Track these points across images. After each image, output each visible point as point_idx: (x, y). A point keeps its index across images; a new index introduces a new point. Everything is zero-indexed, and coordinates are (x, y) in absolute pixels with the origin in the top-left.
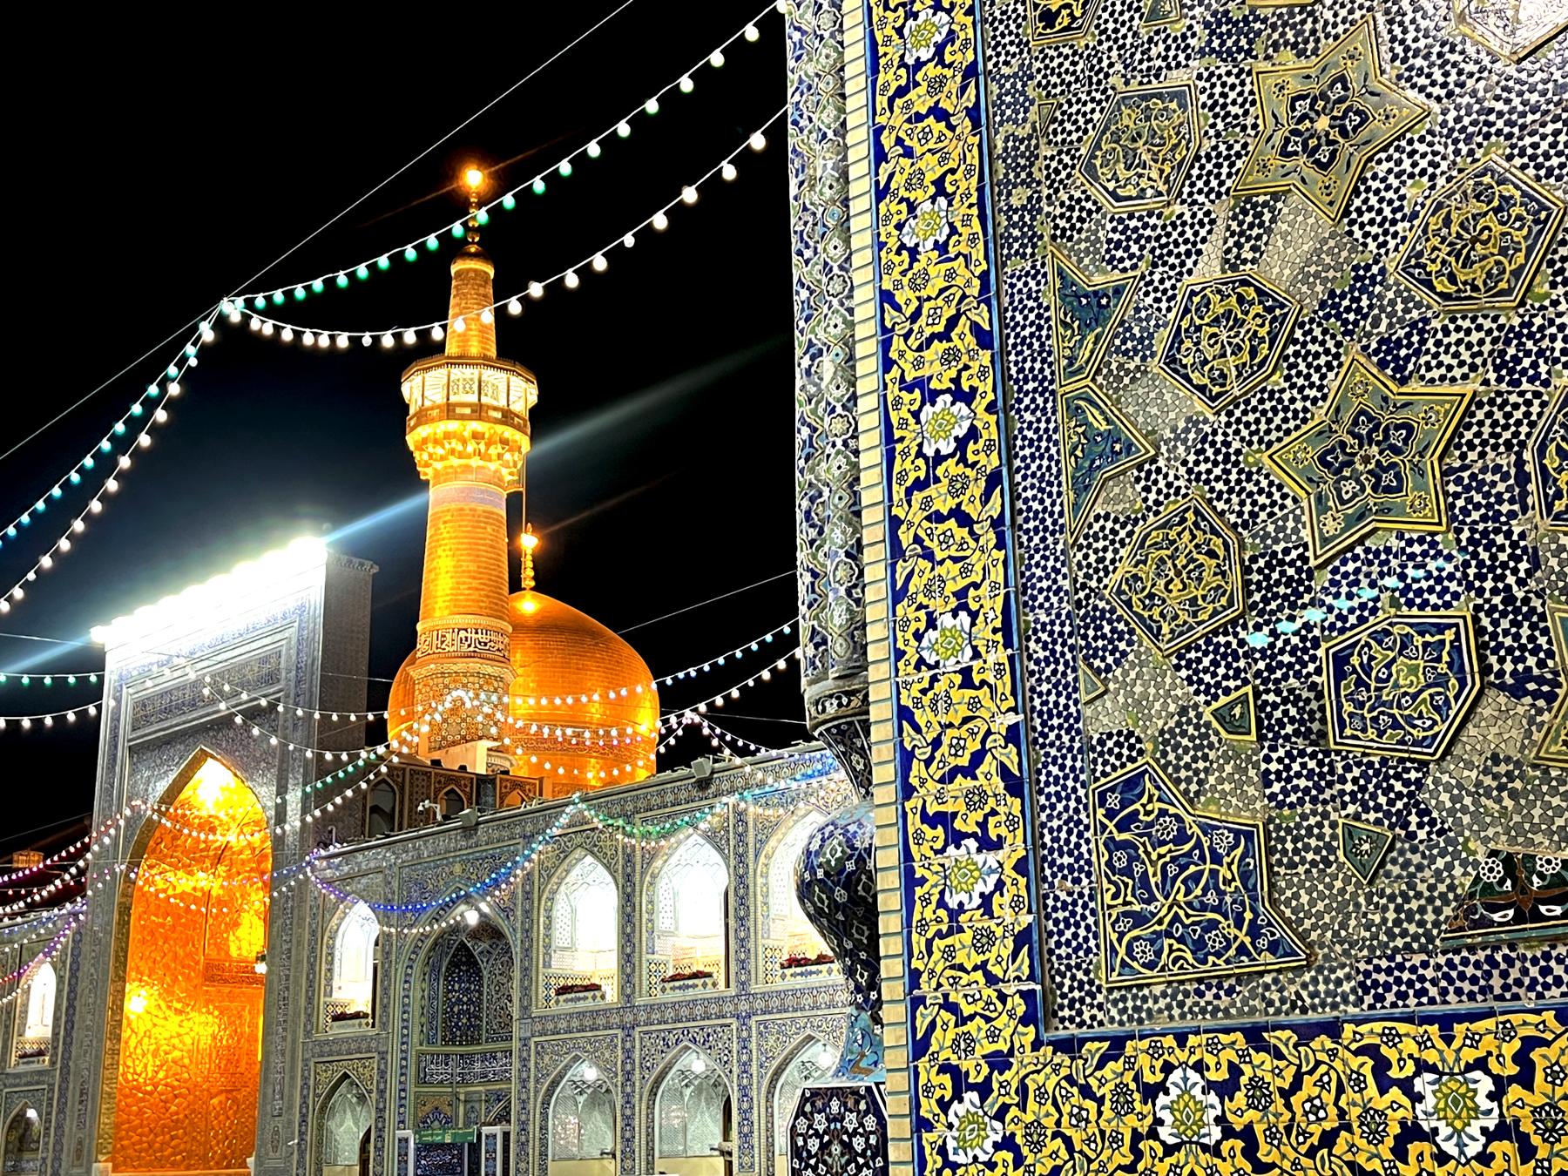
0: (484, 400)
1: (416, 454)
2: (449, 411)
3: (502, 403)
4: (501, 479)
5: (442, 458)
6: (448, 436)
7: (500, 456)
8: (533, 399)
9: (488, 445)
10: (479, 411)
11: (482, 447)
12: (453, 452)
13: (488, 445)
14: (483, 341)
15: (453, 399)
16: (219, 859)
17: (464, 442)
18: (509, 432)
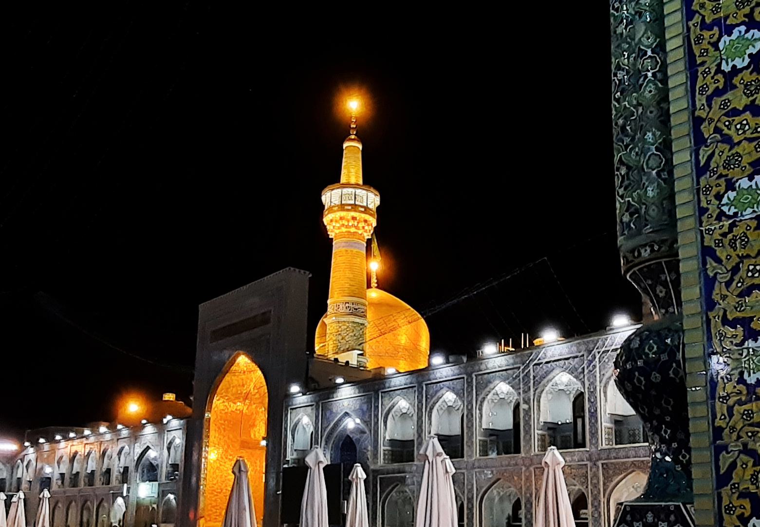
0: (357, 203)
1: (328, 227)
2: (342, 207)
3: (365, 204)
4: (364, 237)
5: (339, 228)
6: (341, 218)
7: (363, 227)
8: (378, 203)
9: (358, 223)
10: (354, 207)
11: (356, 224)
12: (343, 225)
13: (358, 223)
14: (357, 177)
15: (343, 202)
16: (246, 398)
17: (348, 221)
18: (367, 217)
